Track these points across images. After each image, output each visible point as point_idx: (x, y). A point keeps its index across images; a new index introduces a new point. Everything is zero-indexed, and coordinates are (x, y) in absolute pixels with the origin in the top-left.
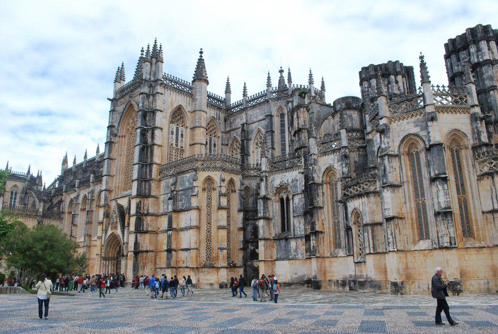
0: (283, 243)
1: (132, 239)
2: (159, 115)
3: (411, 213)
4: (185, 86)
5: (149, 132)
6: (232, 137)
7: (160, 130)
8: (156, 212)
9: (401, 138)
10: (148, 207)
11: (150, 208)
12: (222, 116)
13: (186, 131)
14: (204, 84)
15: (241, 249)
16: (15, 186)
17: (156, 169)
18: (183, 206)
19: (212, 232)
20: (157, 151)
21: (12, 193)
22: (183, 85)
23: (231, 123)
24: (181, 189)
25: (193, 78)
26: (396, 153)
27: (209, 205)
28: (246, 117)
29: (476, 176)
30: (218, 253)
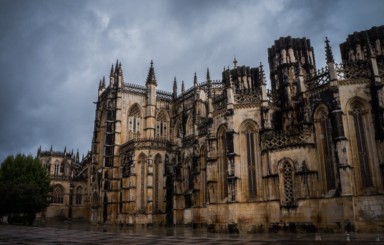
2: (118, 113)
3: (221, 178)
5: (113, 124)
7: (119, 123)
8: (117, 178)
9: (218, 127)
10: (112, 174)
11: (113, 175)
12: (171, 106)
13: (141, 120)
14: (153, 86)
17: (117, 149)
20: (117, 137)
21: (56, 165)
25: (146, 82)
28: (184, 106)
29: (260, 152)
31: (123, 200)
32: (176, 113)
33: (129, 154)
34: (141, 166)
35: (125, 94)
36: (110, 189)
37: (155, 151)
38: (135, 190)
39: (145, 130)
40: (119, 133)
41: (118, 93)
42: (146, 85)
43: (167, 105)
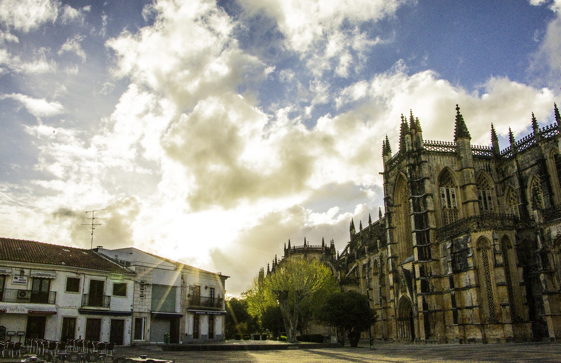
1: (420, 300)
2: (427, 183)
4: (448, 147)
6: (507, 188)
10: (431, 271)
11: (432, 271)
12: (493, 166)
15: (526, 304)
18: (461, 267)
20: (431, 217)
23: (503, 172)
24: (457, 251)
27: (486, 264)
28: (518, 165)
30: (501, 309)
31: (458, 305)
32: (503, 176)
33: (458, 240)
34: (481, 254)
36: (429, 291)
39: (465, 203)
40: (431, 212)
41: (422, 156)
42: (455, 140)
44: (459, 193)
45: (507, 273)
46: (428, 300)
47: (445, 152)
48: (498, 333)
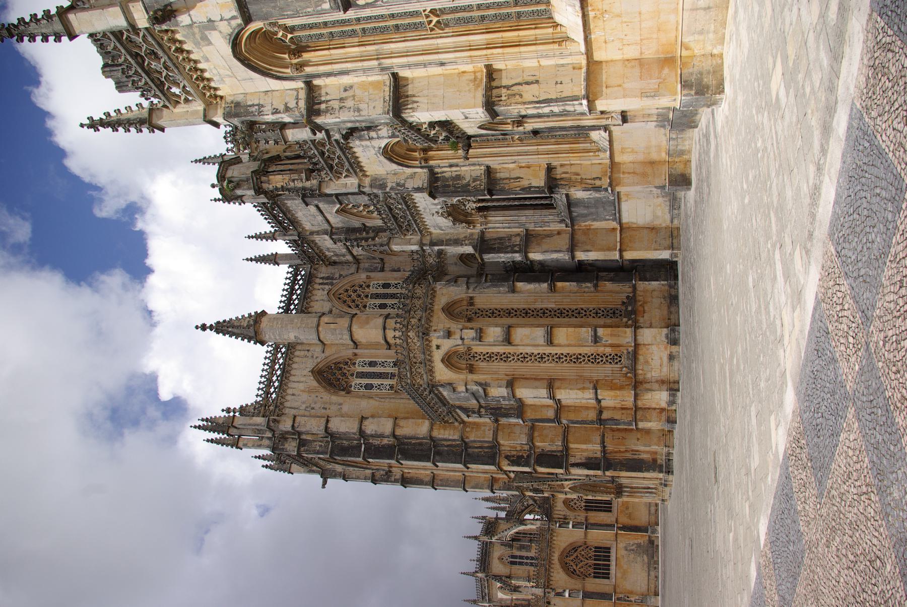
0: (577, 211)
7: (366, 423)
12: (324, 271)
15: (596, 286)
16: (501, 559)
17: (442, 431)
19: (559, 352)
21: (512, 563)
22: (272, 368)
23: (336, 255)
25: (255, 343)
26: (300, 84)
27: (504, 357)
32: (344, 256)
35: (287, 404)
36: (562, 451)
37: (435, 319)
38: (557, 384)
39: (389, 346)
40: (395, 425)
42: (263, 343)
43: (321, 281)
44: (366, 351)
45: (527, 314)
46: (577, 458)
47: (284, 371)
48: (655, 357)
